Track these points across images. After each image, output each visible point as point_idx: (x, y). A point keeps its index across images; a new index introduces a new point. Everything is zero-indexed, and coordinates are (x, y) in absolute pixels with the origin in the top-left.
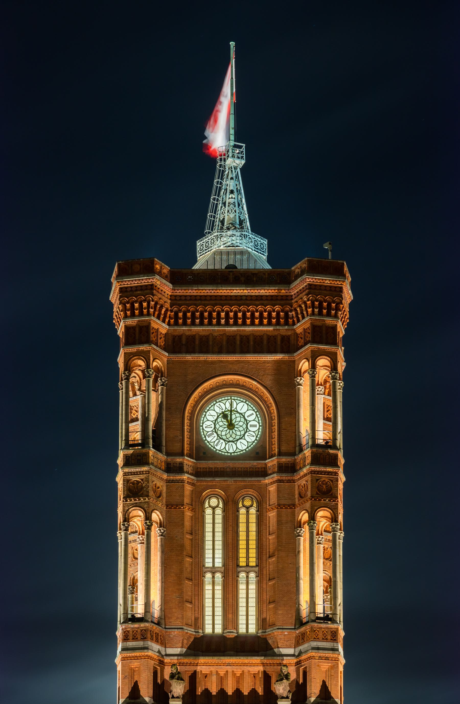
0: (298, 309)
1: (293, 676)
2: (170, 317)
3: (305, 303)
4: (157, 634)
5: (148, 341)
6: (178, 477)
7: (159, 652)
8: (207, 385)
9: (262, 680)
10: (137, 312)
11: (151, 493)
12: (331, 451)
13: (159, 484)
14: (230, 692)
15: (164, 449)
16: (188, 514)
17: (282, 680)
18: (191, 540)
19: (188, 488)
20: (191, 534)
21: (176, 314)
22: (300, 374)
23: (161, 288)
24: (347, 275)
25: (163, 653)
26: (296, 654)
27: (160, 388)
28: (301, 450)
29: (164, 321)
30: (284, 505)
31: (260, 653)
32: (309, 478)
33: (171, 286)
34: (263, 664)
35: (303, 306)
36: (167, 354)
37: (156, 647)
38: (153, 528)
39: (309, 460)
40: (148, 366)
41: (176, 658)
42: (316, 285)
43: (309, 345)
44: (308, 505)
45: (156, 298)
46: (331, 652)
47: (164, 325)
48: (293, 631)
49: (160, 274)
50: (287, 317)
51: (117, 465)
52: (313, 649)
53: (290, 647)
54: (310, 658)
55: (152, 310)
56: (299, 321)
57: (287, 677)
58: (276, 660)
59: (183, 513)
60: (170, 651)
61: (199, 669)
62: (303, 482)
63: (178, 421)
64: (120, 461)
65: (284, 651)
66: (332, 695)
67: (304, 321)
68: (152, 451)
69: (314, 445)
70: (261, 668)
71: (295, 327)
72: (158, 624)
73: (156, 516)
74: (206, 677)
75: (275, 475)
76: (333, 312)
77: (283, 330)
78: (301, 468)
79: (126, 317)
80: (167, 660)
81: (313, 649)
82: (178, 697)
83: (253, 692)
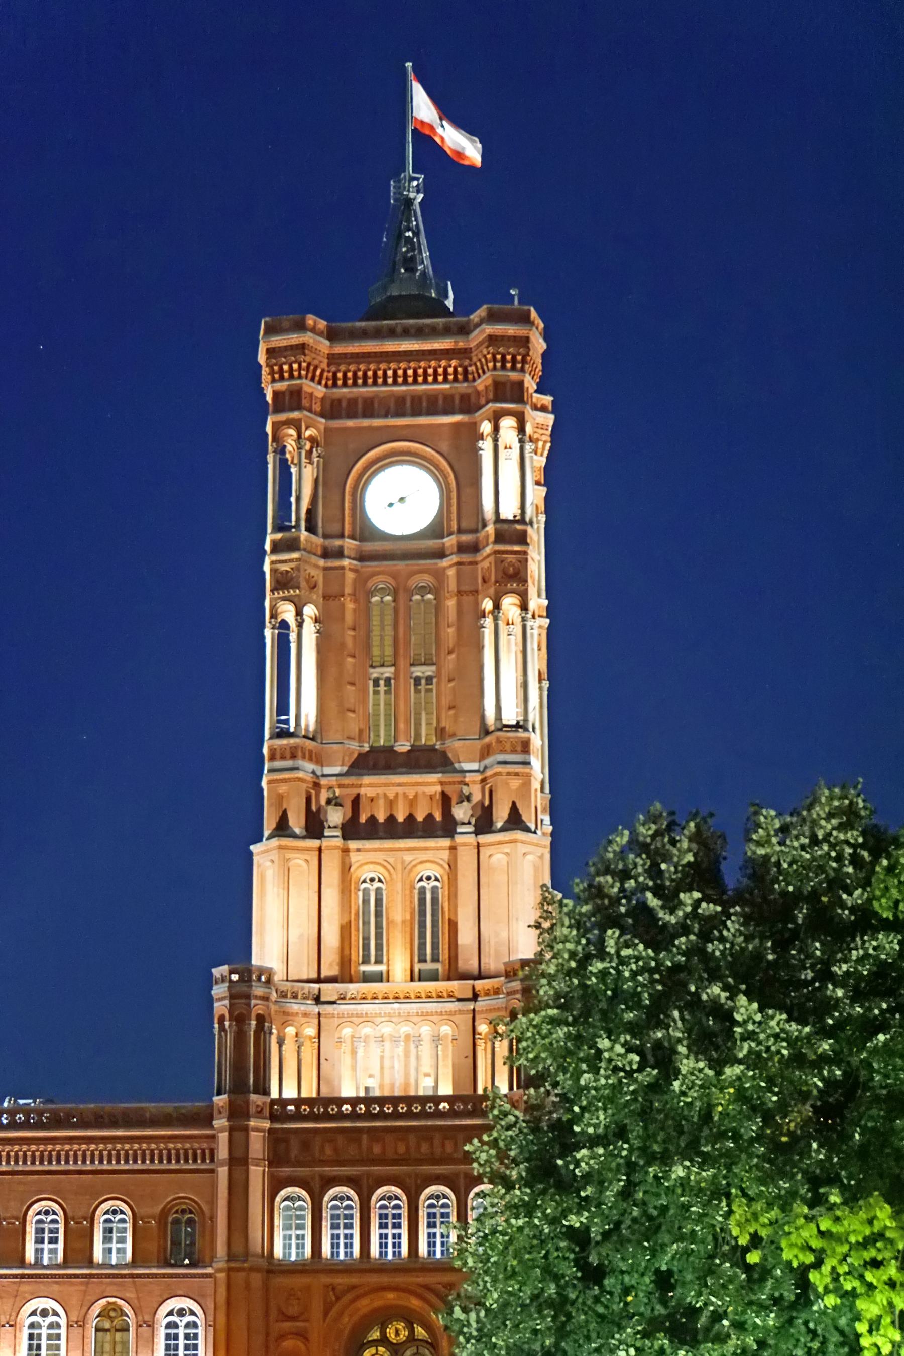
0: (478, 364)
1: (477, 797)
2: (327, 379)
3: (485, 356)
4: (311, 752)
5: (299, 408)
6: (337, 563)
7: (313, 773)
8: (371, 454)
9: (440, 802)
10: (286, 375)
11: (303, 584)
12: (519, 527)
13: (313, 572)
14: (401, 819)
15: (320, 531)
16: (350, 606)
17: (462, 801)
18: (354, 637)
19: (350, 576)
20: (354, 629)
21: (335, 374)
22: (481, 437)
23: (315, 346)
24: (536, 322)
25: (319, 773)
26: (481, 770)
27: (316, 460)
28: (485, 525)
29: (320, 383)
30: (465, 592)
31: (438, 770)
32: (492, 559)
33: (327, 343)
34: (442, 783)
35: (483, 360)
36: (323, 421)
37: (310, 766)
38: (305, 625)
39: (492, 539)
40: (299, 436)
41: (335, 778)
42: (496, 336)
43: (490, 405)
44: (492, 591)
45: (308, 359)
46: (521, 766)
47: (319, 387)
48: (477, 741)
49: (313, 330)
50: (466, 372)
51: (265, 552)
52: (500, 763)
53: (473, 761)
54: (496, 774)
55: (303, 373)
56: (479, 376)
57: (468, 798)
58: (457, 778)
59: (343, 605)
60: (328, 771)
61: (363, 791)
62: (486, 564)
63: (337, 498)
64: (268, 547)
65: (466, 766)
66: (524, 818)
67: (484, 377)
68: (304, 534)
69: (498, 520)
70: (439, 789)
71: (476, 384)
72: (313, 739)
73: (310, 611)
74: (372, 800)
75: (453, 557)
76: (519, 365)
77: (463, 387)
78: (484, 548)
79: (274, 380)
80: (324, 782)
81: (500, 763)
82: (335, 827)
83: (430, 816)
